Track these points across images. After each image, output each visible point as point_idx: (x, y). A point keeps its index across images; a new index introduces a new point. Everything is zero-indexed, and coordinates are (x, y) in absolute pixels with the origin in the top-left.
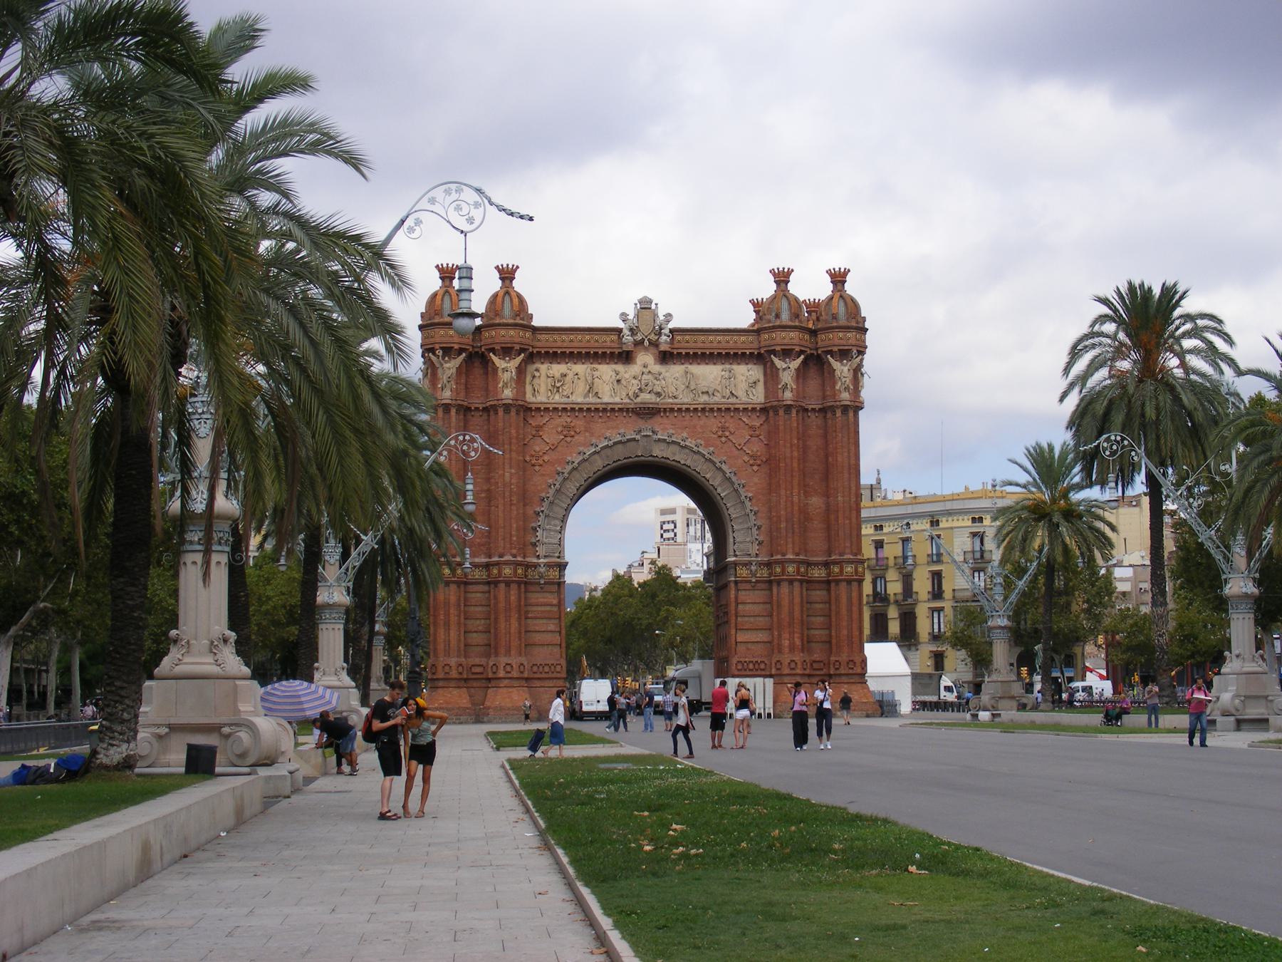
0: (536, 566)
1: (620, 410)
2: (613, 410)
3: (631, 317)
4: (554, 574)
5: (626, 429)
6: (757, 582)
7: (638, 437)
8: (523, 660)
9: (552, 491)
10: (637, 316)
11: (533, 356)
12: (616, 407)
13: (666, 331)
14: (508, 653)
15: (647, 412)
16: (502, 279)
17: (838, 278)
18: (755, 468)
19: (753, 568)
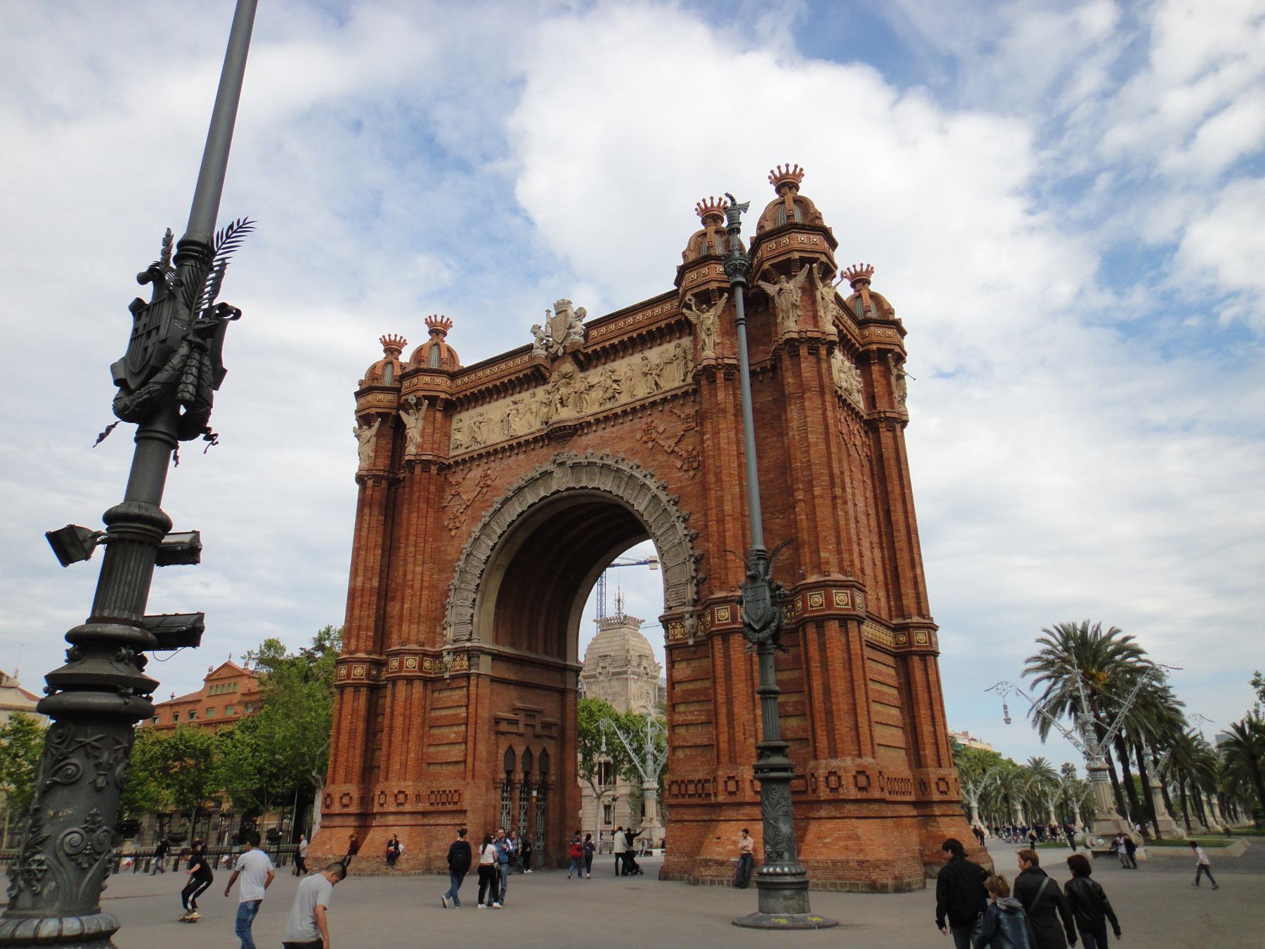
0: (438, 656)
1: (536, 440)
2: (527, 442)
3: (543, 329)
4: (462, 664)
5: (542, 459)
6: (696, 645)
7: (549, 467)
8: (409, 787)
9: (463, 557)
10: (552, 323)
11: (452, 407)
12: (530, 437)
13: (580, 327)
14: (387, 779)
15: (558, 435)
16: (431, 332)
17: (786, 183)
18: (691, 473)
19: (688, 622)
